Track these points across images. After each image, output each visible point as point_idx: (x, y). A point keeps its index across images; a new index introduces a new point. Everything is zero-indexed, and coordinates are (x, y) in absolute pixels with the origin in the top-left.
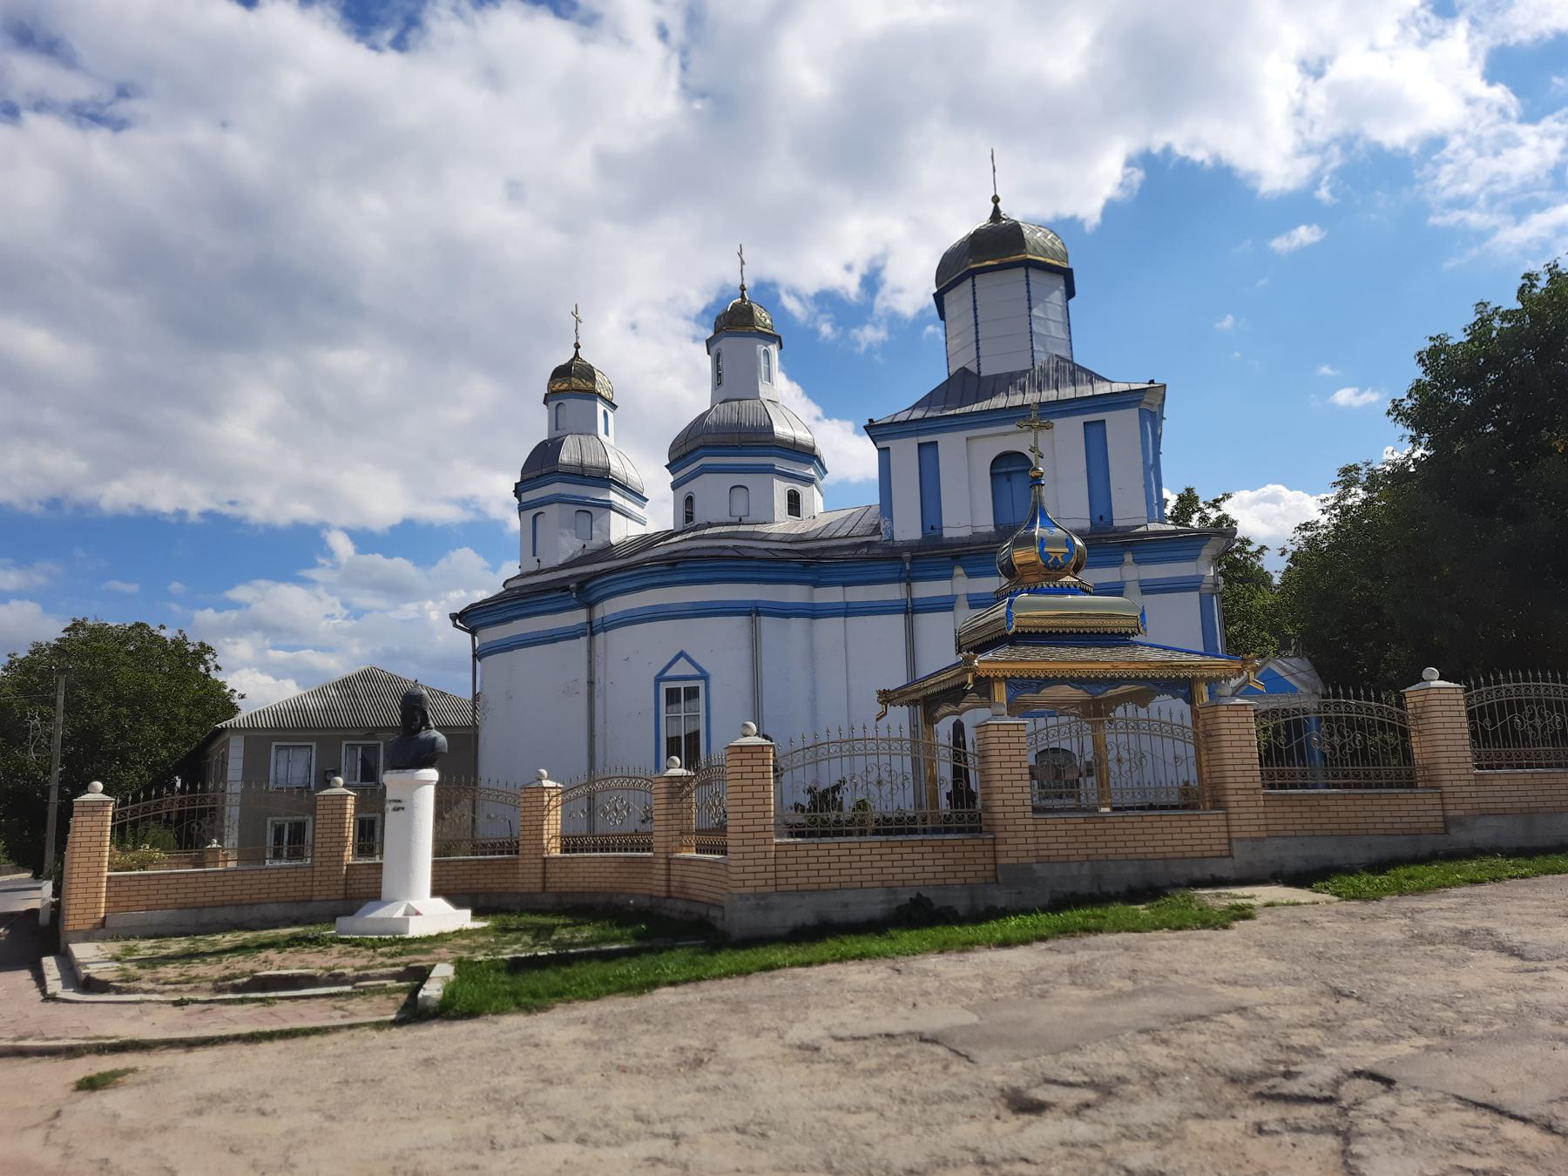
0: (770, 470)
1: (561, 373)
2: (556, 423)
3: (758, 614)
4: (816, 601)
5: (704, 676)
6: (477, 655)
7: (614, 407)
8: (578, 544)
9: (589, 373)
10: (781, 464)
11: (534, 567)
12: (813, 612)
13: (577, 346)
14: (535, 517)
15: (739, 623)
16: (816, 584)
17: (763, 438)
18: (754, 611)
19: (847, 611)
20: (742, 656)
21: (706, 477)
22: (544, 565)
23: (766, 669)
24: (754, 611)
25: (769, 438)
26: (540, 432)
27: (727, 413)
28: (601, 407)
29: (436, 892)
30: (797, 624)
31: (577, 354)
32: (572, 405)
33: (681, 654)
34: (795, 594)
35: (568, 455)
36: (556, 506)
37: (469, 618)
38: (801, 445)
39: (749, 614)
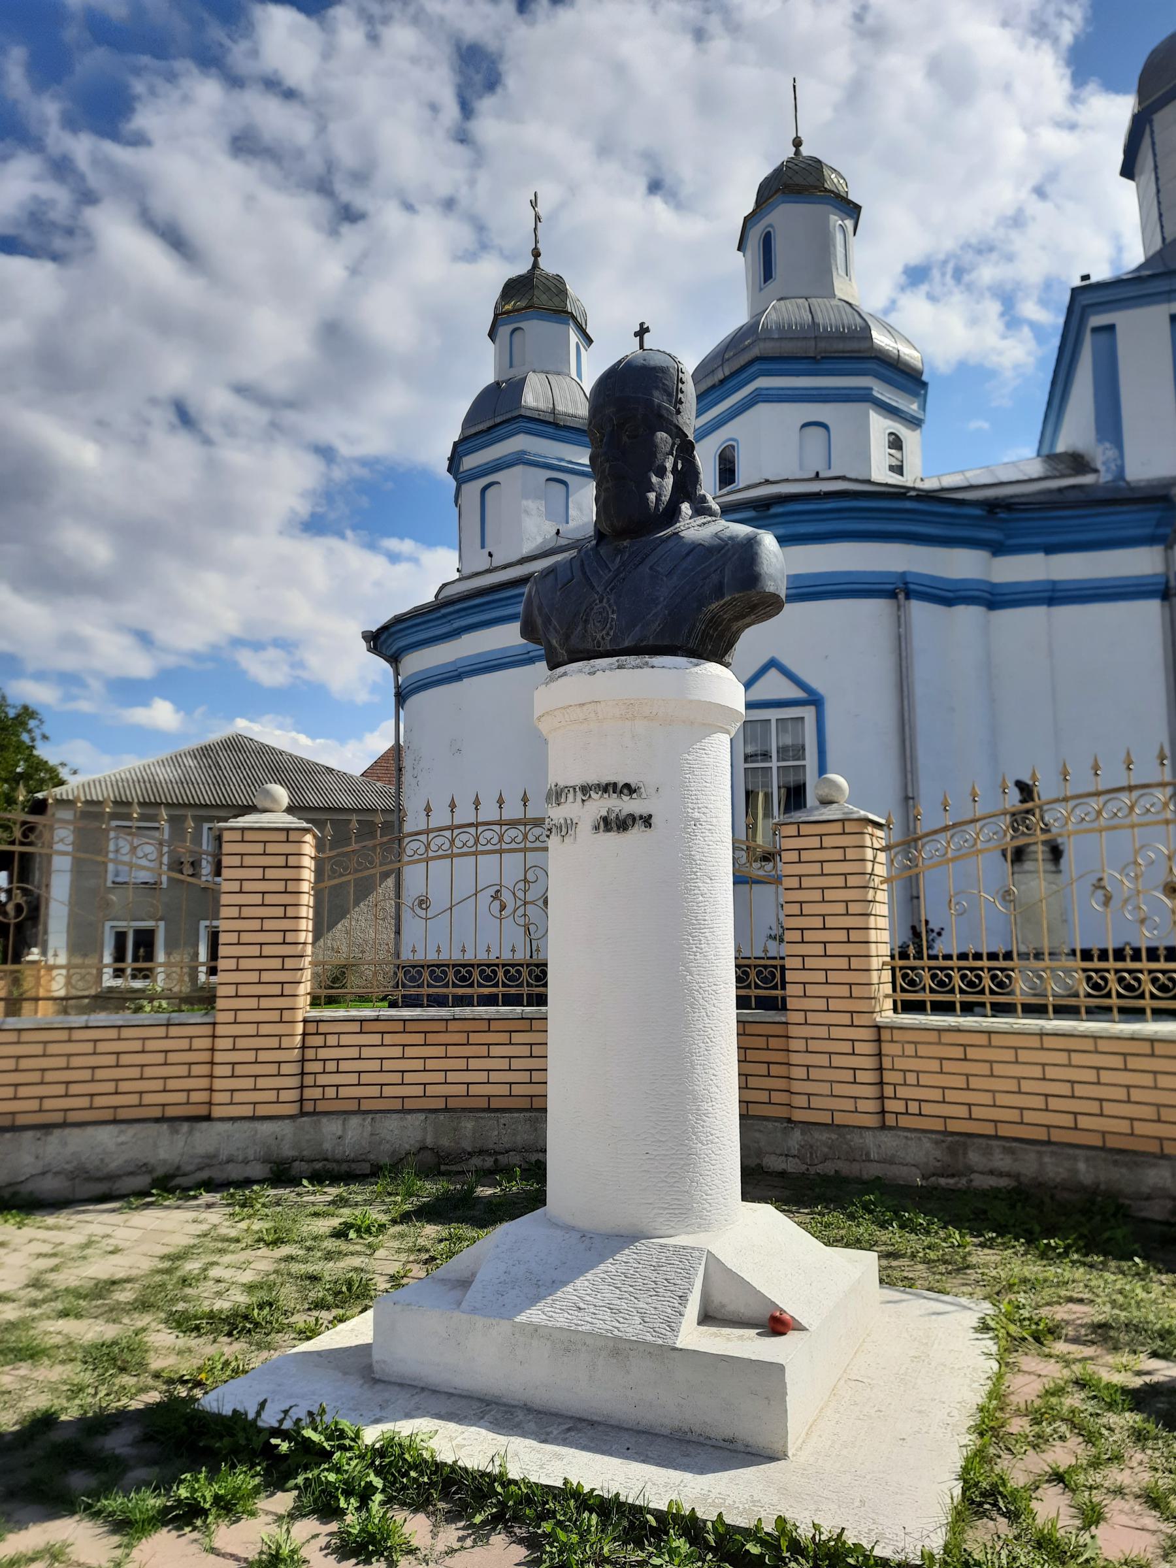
0: (864, 397)
1: (515, 289)
2: (509, 357)
3: (908, 595)
4: (996, 579)
5: (815, 700)
6: (401, 697)
7: (589, 340)
8: (549, 529)
9: (557, 288)
10: (882, 392)
11: (483, 563)
12: (995, 598)
13: (536, 254)
14: (484, 490)
15: (872, 612)
16: (998, 549)
17: (855, 345)
18: (899, 590)
19: (1054, 595)
20: (877, 664)
21: (762, 409)
22: (498, 561)
23: (921, 690)
24: (899, 590)
25: (864, 345)
26: (483, 369)
27: (784, 312)
28: (574, 338)
29: (748, 1195)
30: (968, 615)
31: (535, 265)
32: (536, 329)
33: (772, 664)
34: (962, 564)
35: (533, 397)
36: (518, 469)
37: (386, 641)
38: (906, 364)
39: (892, 595)
